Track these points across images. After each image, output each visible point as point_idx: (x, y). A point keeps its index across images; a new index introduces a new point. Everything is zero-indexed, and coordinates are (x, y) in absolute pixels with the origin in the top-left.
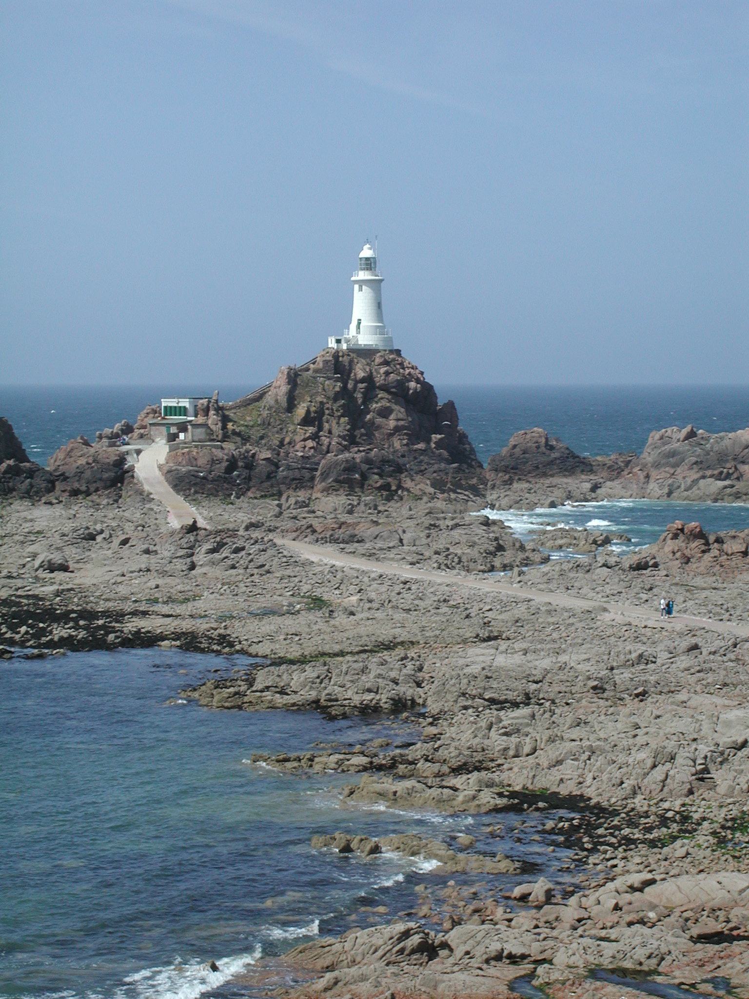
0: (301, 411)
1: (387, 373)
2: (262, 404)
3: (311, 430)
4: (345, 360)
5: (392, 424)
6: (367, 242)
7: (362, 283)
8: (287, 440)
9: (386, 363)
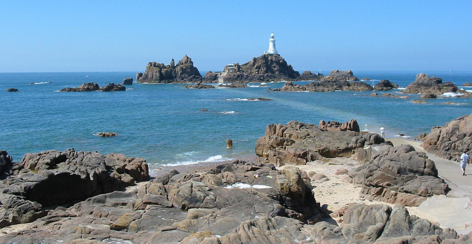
0: (256, 66)
1: (275, 59)
2: (248, 65)
3: (257, 70)
4: (266, 56)
5: (276, 69)
6: (273, 33)
7: (271, 41)
8: (252, 72)
9: (275, 57)
